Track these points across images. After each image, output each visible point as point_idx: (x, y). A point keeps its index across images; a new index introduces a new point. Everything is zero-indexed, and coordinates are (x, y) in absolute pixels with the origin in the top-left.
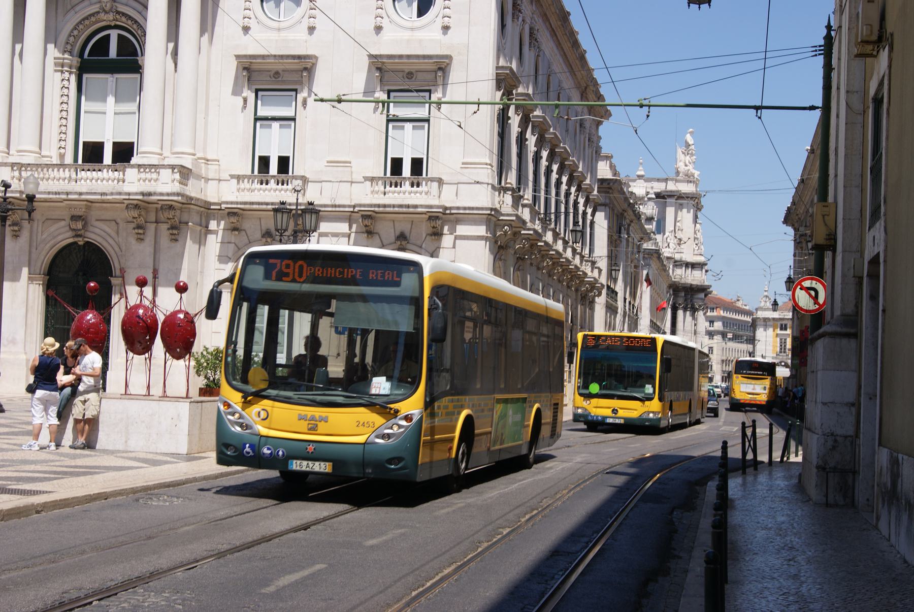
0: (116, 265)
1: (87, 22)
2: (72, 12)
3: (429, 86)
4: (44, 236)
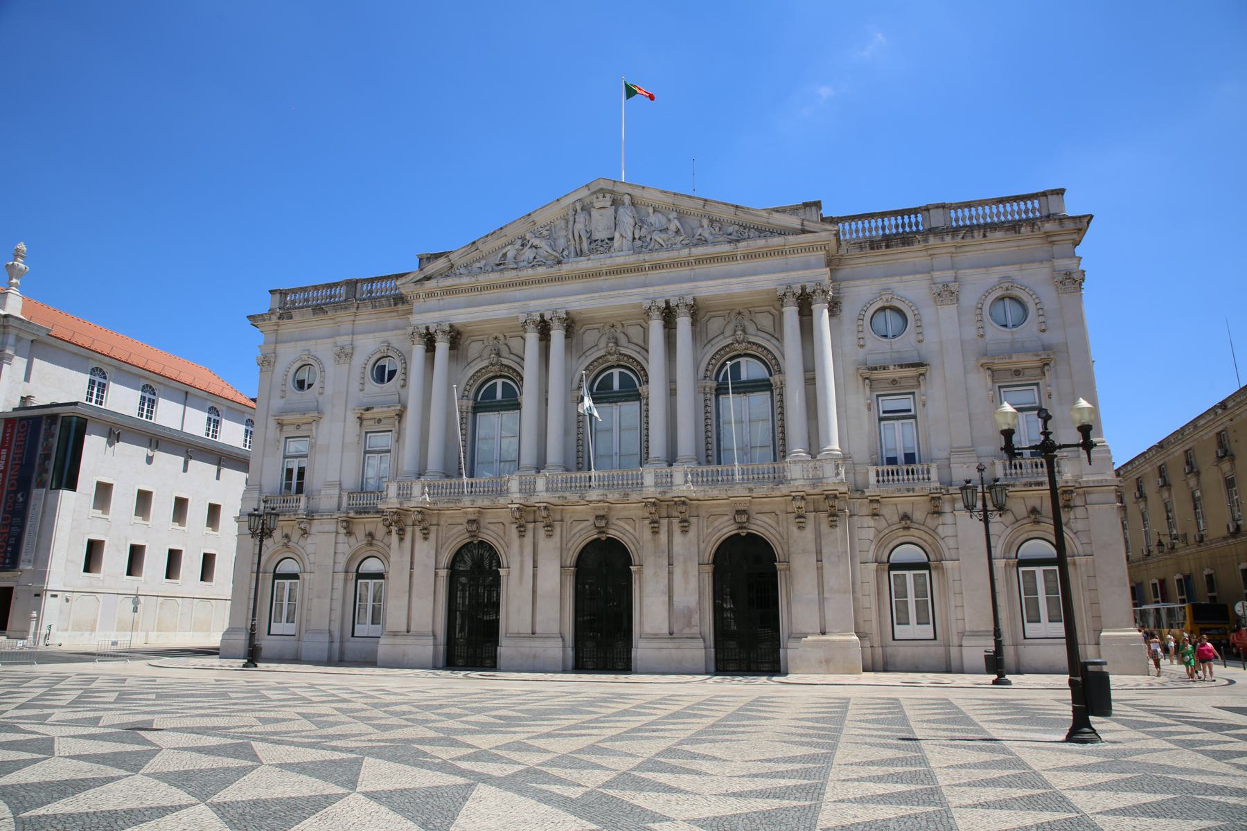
0: (779, 551)
1: (722, 352)
2: (709, 345)
3: (1036, 379)
4: (710, 530)
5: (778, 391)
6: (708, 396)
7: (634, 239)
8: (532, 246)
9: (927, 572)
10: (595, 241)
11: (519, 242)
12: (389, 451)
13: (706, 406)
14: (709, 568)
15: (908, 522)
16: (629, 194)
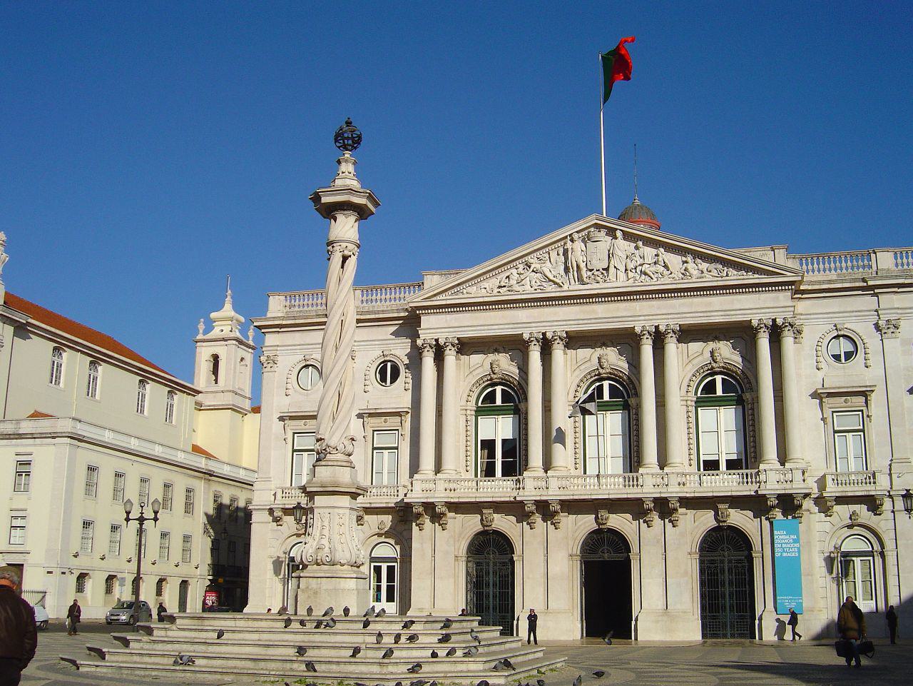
5: (750, 406)
6: (690, 408)
7: (626, 270)
8: (533, 271)
9: (871, 558)
10: (591, 270)
11: (521, 267)
12: (397, 448)
13: (688, 417)
14: (697, 556)
15: (857, 517)
16: (620, 230)
